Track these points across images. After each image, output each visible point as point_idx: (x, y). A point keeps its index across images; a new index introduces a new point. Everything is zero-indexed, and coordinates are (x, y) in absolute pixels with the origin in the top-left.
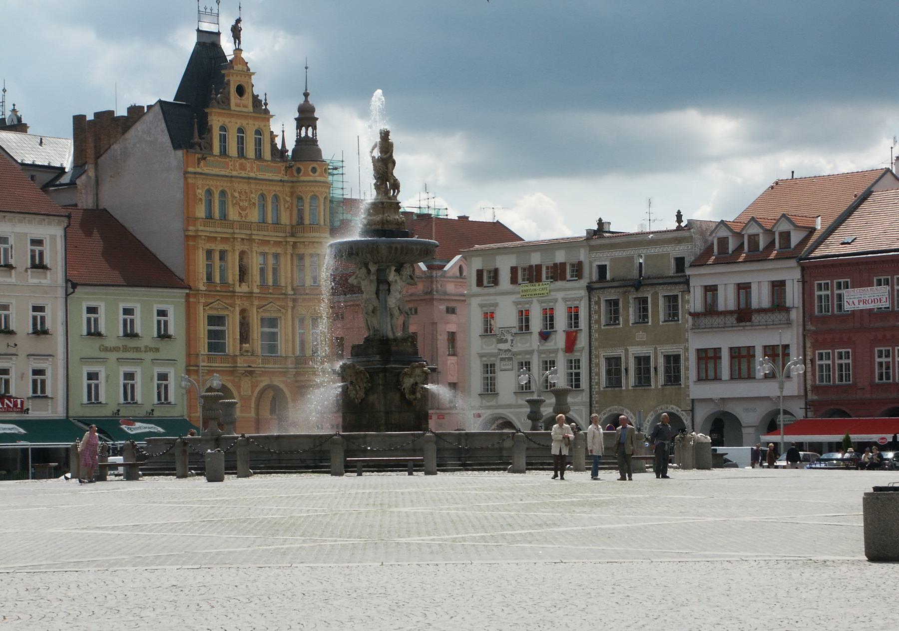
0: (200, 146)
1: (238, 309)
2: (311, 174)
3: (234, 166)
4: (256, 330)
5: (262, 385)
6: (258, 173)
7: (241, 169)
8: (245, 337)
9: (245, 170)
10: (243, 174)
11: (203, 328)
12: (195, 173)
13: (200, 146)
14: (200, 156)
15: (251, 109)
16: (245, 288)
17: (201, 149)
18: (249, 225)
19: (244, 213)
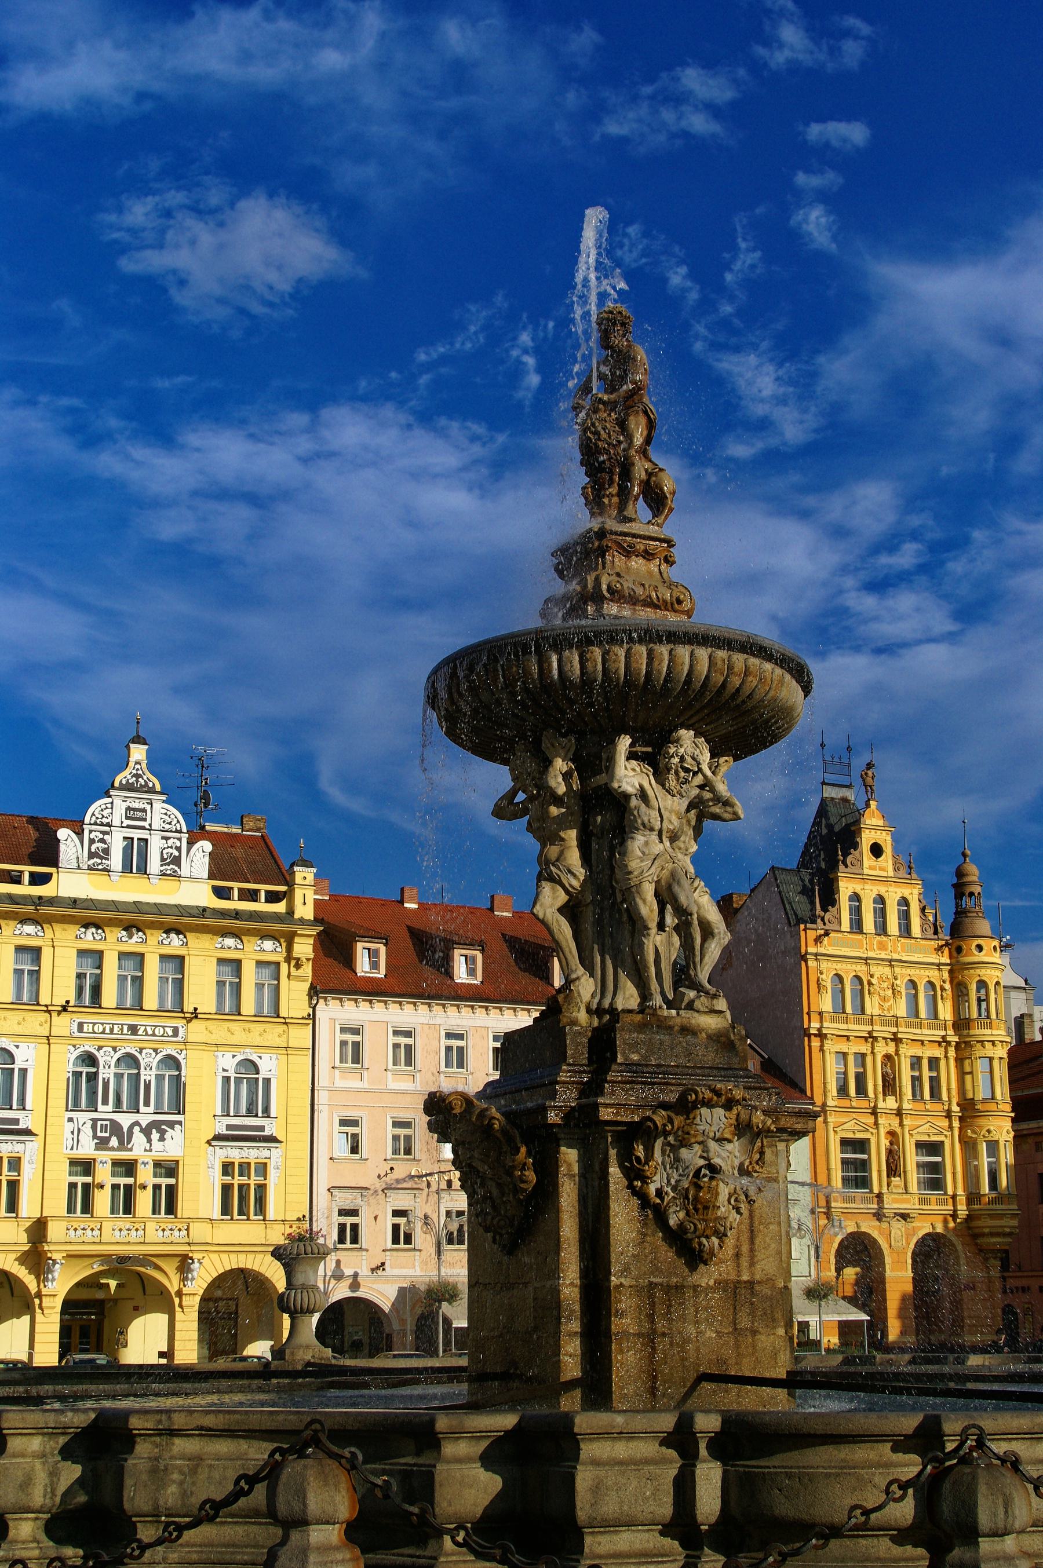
0: (823, 919)
1: (883, 1132)
2: (976, 953)
3: (872, 944)
4: (912, 1159)
5: (921, 1234)
6: (903, 954)
7: (880, 949)
8: (894, 1168)
9: (886, 950)
10: (883, 956)
11: (836, 1155)
12: (816, 955)
13: (823, 919)
14: (822, 932)
15: (891, 873)
16: (891, 1103)
17: (824, 924)
18: (896, 1021)
19: (886, 1005)
